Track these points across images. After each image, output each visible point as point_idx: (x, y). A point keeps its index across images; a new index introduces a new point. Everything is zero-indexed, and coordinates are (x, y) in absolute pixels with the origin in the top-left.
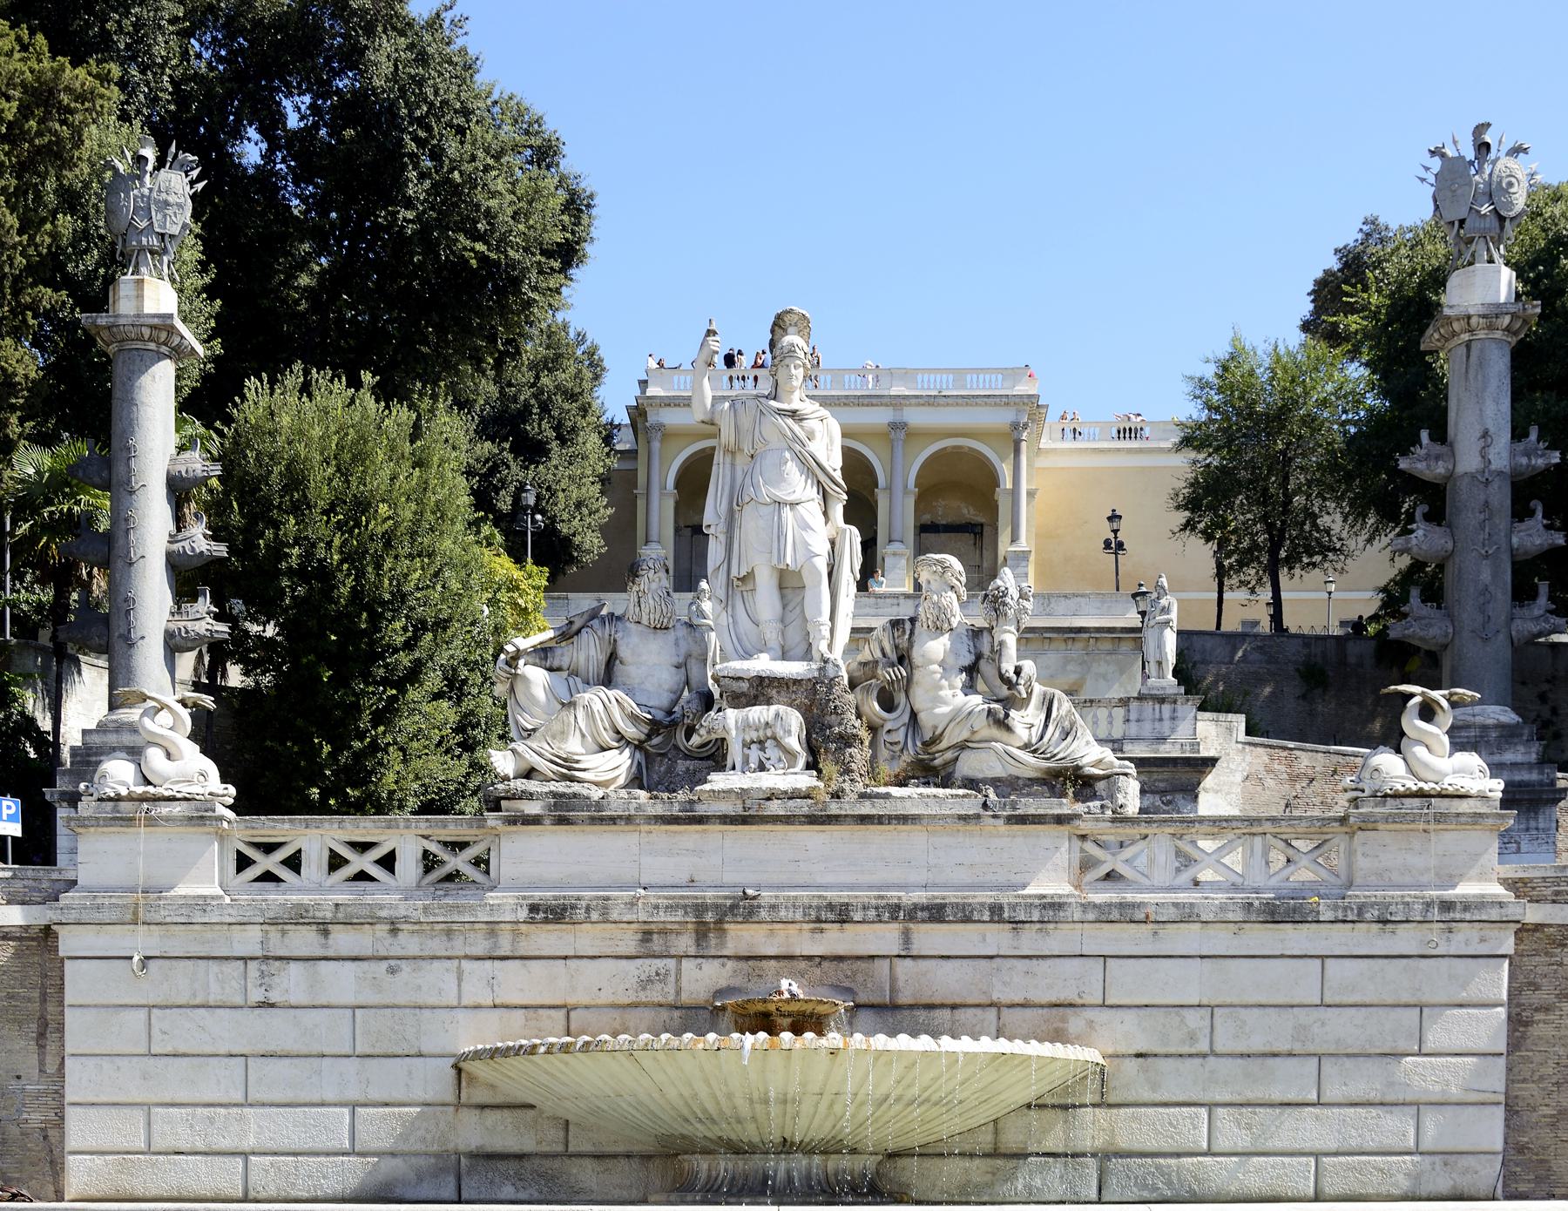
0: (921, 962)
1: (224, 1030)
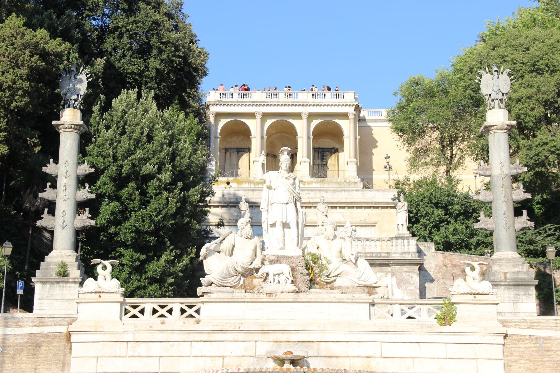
0: (327, 343)
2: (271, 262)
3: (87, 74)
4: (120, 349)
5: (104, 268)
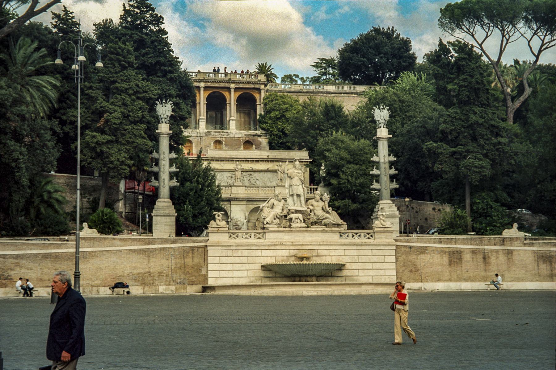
1: (230, 260)
2: (293, 213)
3: (171, 104)
4: (229, 253)
5: (219, 216)
